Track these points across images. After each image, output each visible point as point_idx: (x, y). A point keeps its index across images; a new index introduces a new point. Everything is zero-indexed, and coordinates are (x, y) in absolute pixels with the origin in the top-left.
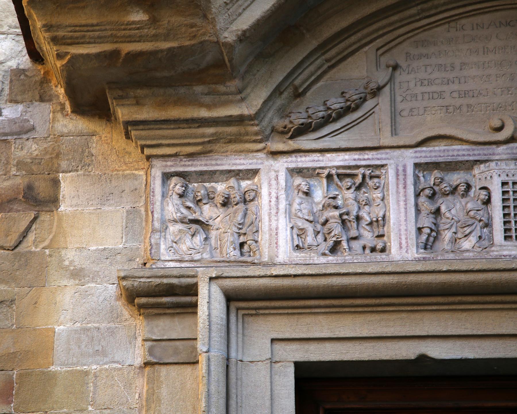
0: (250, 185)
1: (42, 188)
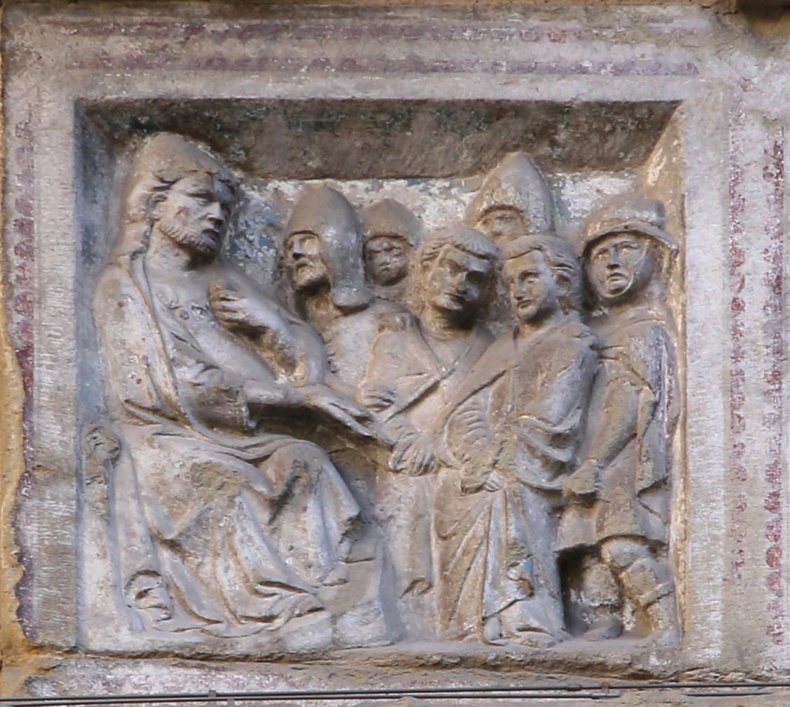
0: (618, 201)
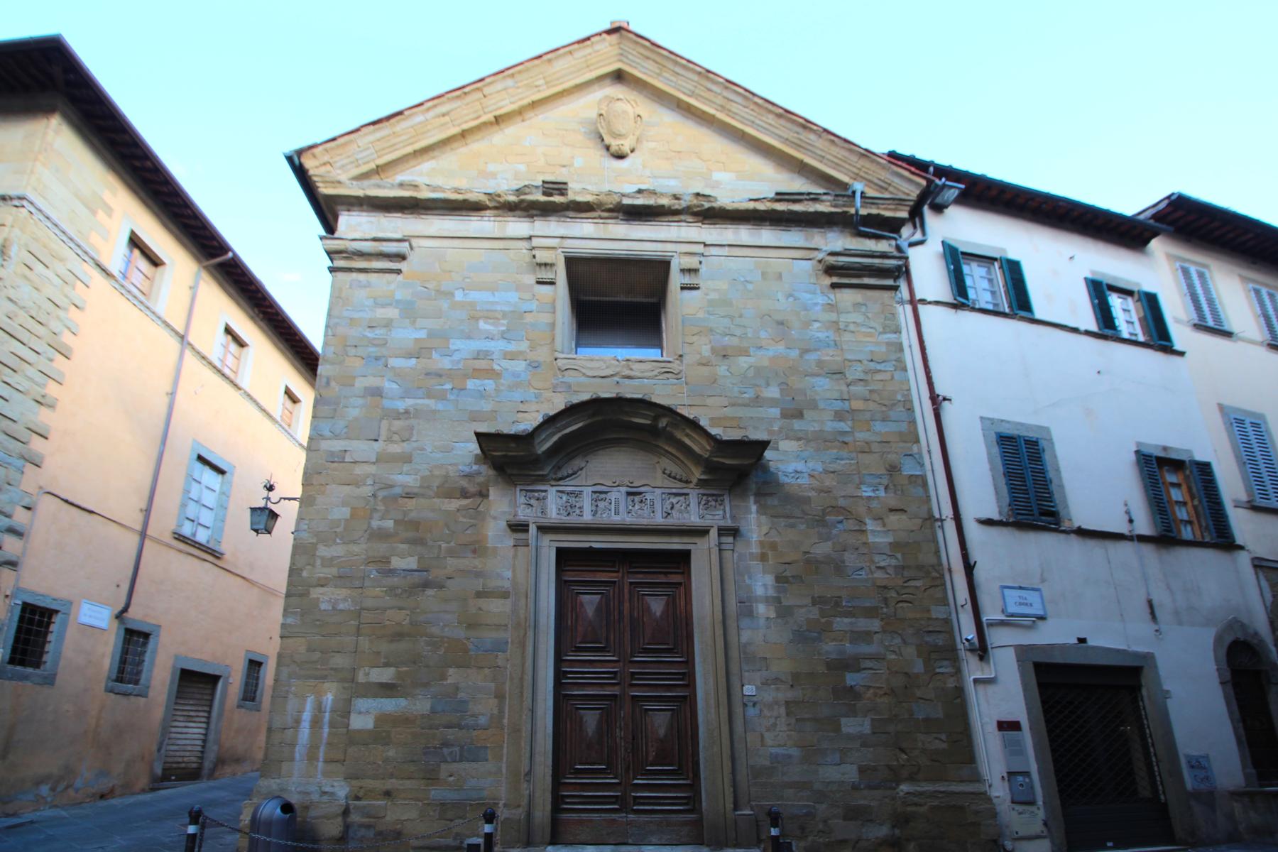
1: (484, 492)
